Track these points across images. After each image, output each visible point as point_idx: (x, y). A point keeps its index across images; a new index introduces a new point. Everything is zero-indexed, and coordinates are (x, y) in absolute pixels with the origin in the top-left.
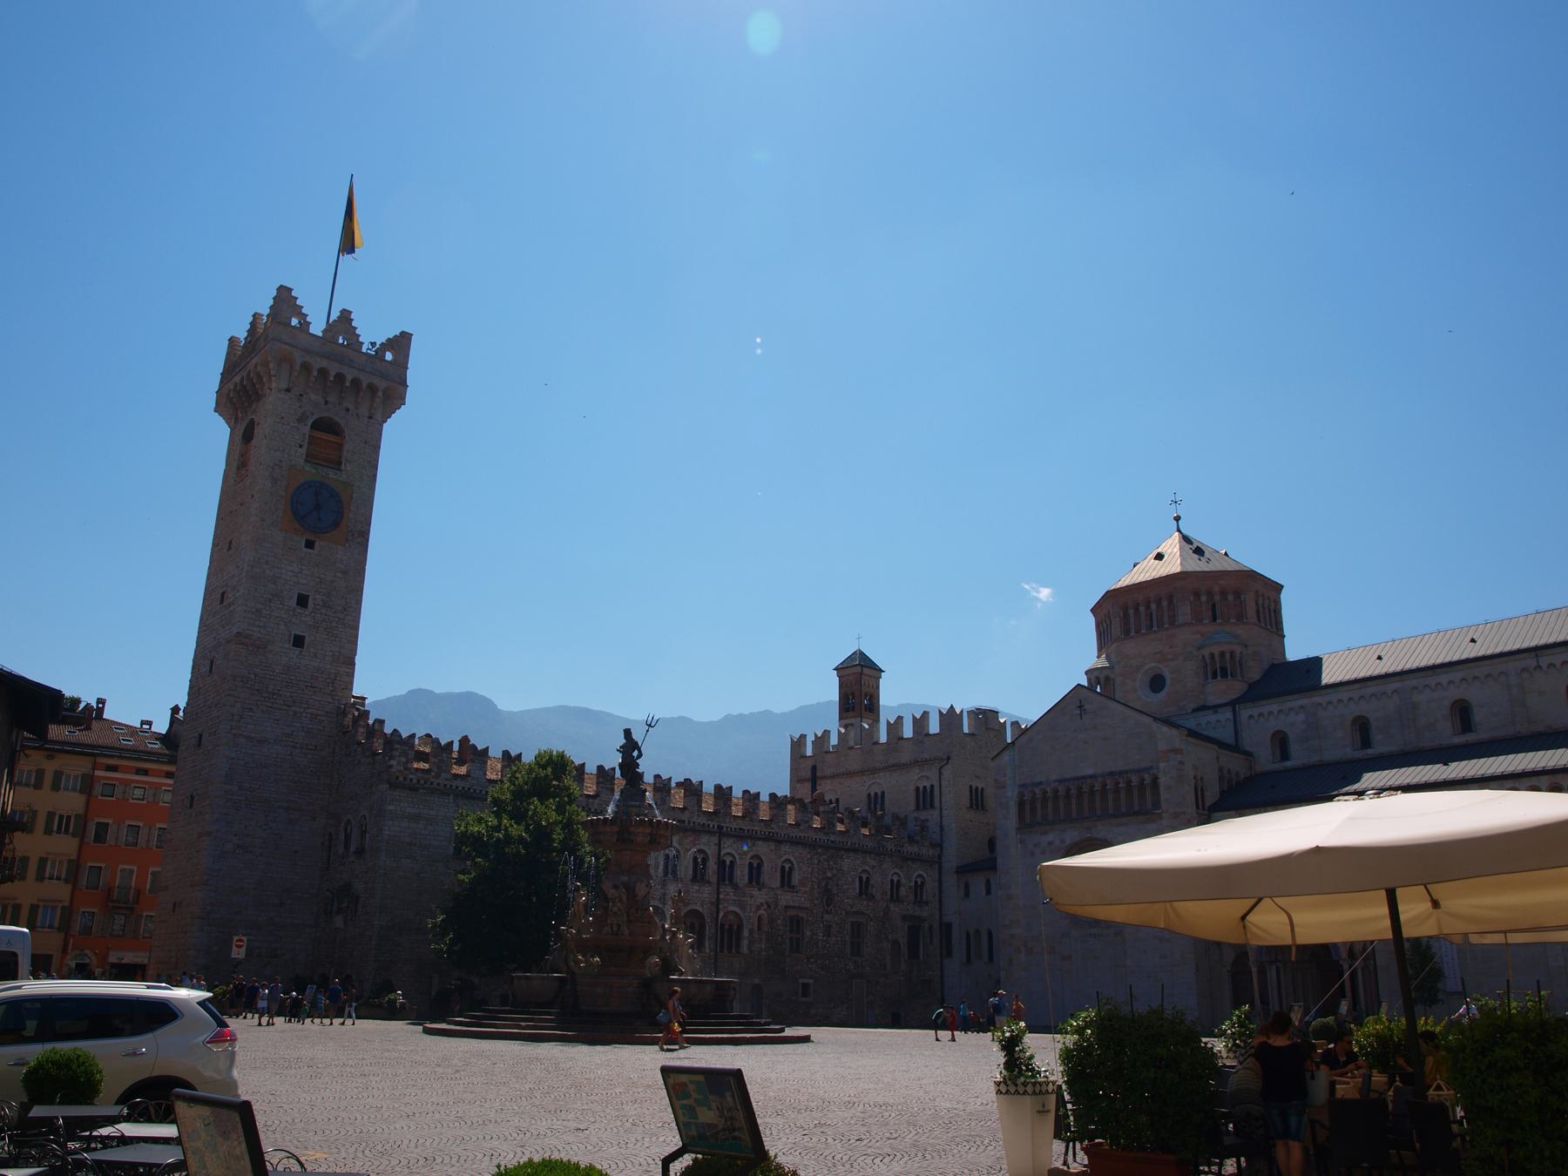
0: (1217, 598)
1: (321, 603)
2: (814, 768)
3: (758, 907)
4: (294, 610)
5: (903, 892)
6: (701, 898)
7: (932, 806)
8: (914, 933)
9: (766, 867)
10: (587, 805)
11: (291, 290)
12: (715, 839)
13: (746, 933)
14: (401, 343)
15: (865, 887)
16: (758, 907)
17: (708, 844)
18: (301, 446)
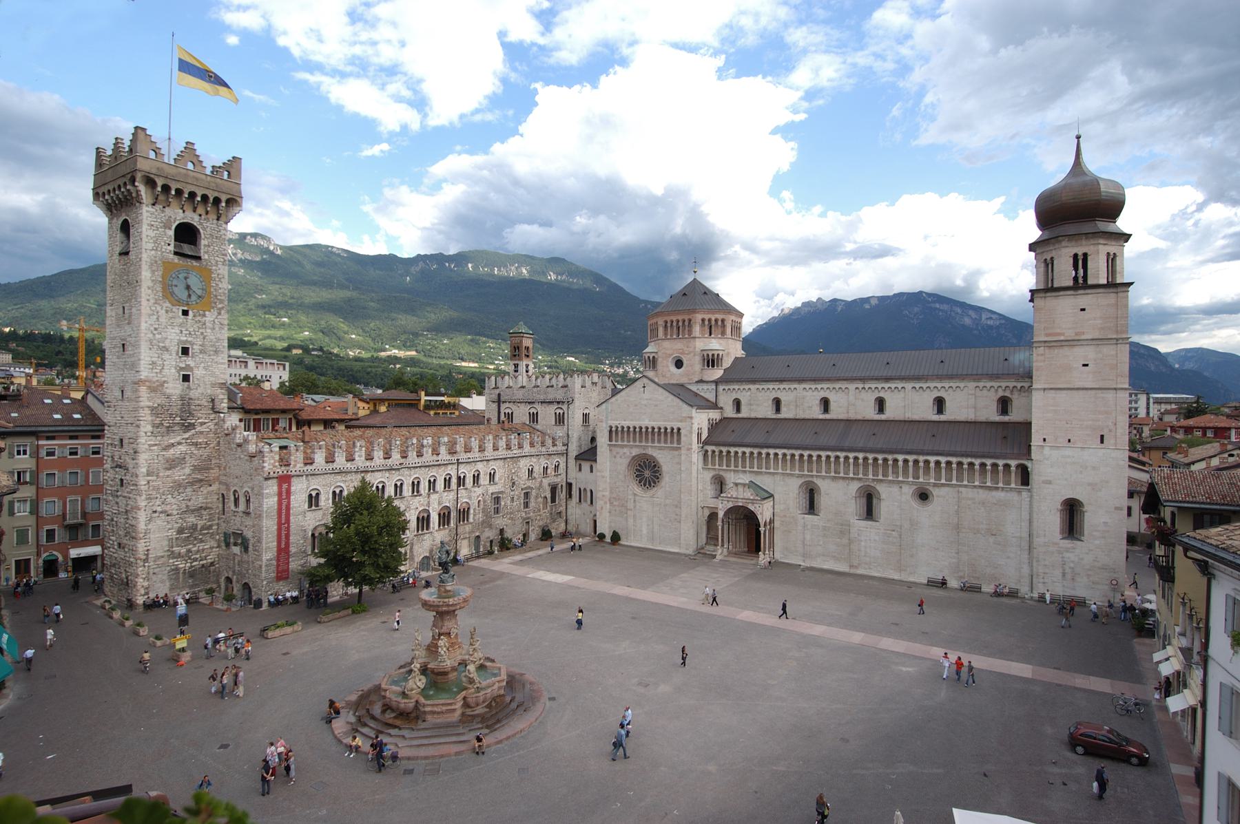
0: (713, 323)
2: (499, 395)
3: (478, 497)
5: (549, 471)
6: (448, 499)
7: (563, 422)
8: (554, 489)
9: (481, 476)
12: (455, 467)
13: (472, 511)
14: (233, 166)
15: (531, 472)
16: (478, 497)
17: (452, 470)
18: (169, 245)
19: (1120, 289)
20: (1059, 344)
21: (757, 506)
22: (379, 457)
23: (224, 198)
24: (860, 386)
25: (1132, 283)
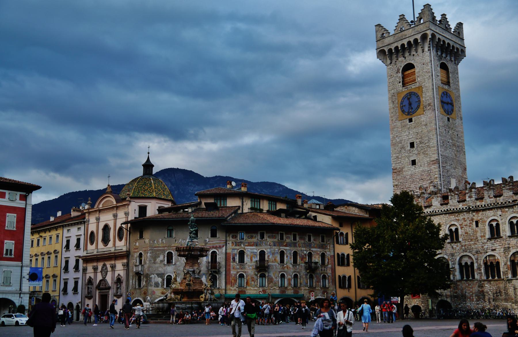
1: (419, 143)
4: (410, 150)
10: (496, 201)
11: (430, 6)
18: (400, 82)
22: (489, 196)
23: (418, 37)
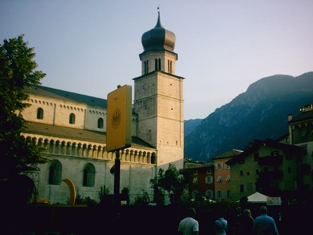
19: (181, 80)
20: (164, 97)
21: (34, 174)
24: (63, 104)
25: (184, 78)
